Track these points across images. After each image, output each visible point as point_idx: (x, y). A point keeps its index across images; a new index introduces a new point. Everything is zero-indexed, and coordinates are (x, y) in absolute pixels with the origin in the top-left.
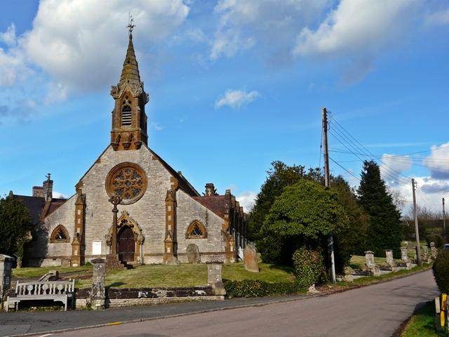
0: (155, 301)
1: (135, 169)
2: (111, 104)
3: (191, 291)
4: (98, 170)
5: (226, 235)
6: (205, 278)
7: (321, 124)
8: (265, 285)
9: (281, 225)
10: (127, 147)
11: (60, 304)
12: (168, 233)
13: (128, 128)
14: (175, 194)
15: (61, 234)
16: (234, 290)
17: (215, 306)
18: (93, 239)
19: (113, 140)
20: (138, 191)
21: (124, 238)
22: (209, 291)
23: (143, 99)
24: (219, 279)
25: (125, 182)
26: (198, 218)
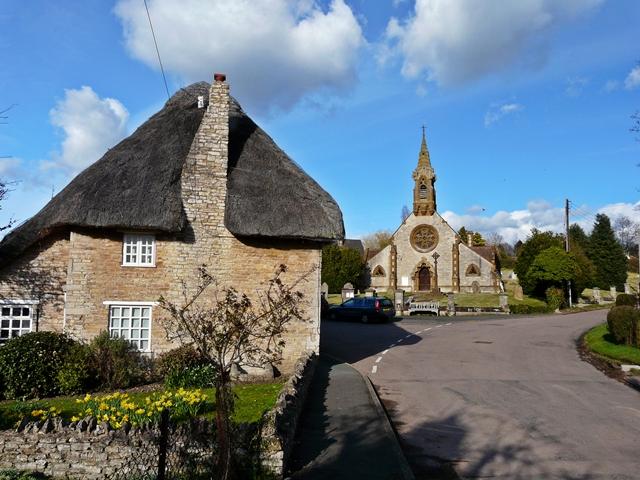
0: (475, 314)
1: (430, 229)
2: (412, 185)
3: (492, 309)
4: (404, 230)
5: (494, 275)
6: (498, 302)
7: (564, 210)
8: (530, 308)
9: (540, 274)
10: (424, 214)
11: (435, 313)
12: (454, 272)
13: (425, 201)
14: (457, 248)
15: (380, 272)
16: (515, 310)
17: (505, 317)
18: (402, 274)
19: (415, 208)
20: (432, 243)
21: (423, 275)
22: (501, 310)
23: (433, 180)
24: (506, 303)
25: (424, 237)
26: (474, 263)
